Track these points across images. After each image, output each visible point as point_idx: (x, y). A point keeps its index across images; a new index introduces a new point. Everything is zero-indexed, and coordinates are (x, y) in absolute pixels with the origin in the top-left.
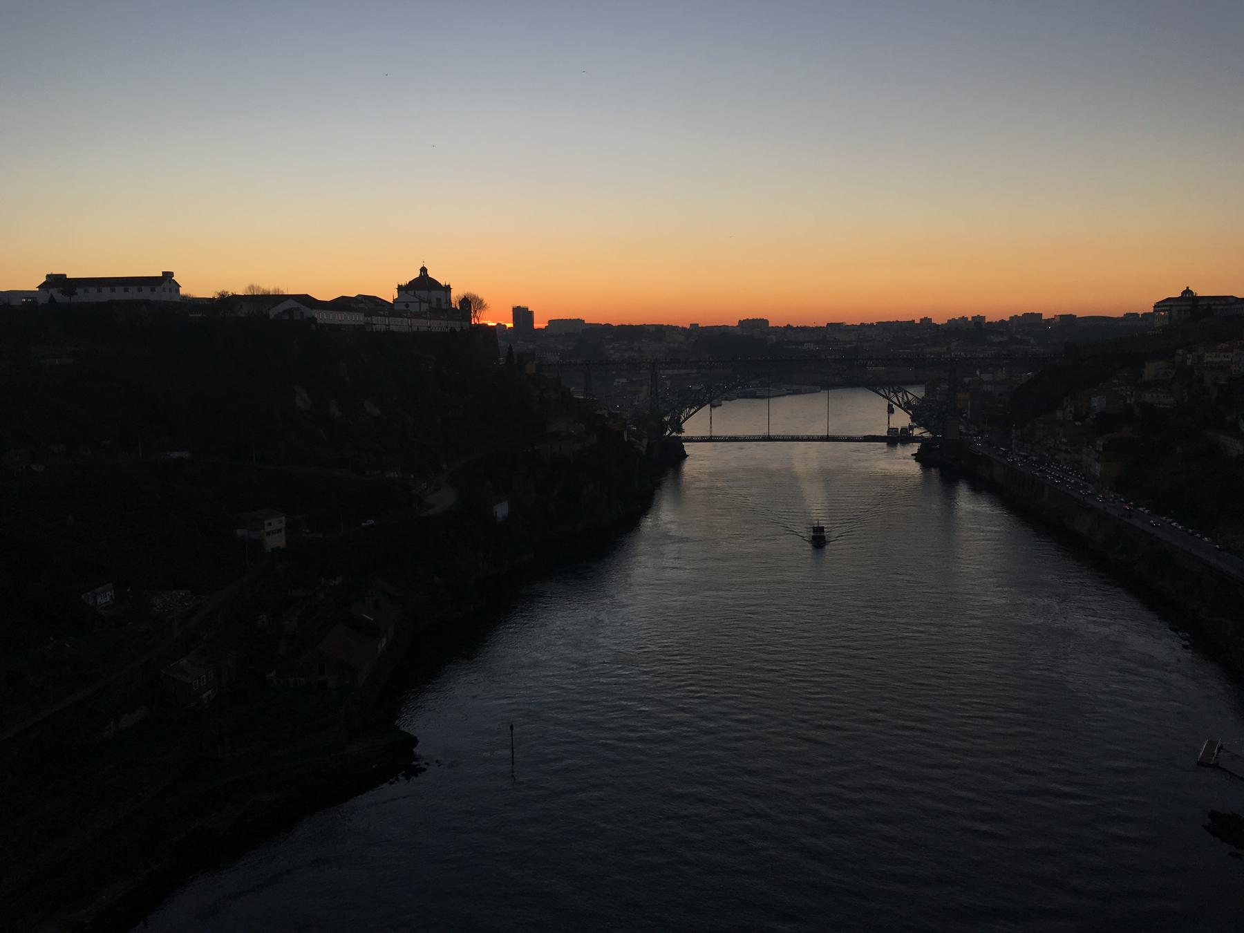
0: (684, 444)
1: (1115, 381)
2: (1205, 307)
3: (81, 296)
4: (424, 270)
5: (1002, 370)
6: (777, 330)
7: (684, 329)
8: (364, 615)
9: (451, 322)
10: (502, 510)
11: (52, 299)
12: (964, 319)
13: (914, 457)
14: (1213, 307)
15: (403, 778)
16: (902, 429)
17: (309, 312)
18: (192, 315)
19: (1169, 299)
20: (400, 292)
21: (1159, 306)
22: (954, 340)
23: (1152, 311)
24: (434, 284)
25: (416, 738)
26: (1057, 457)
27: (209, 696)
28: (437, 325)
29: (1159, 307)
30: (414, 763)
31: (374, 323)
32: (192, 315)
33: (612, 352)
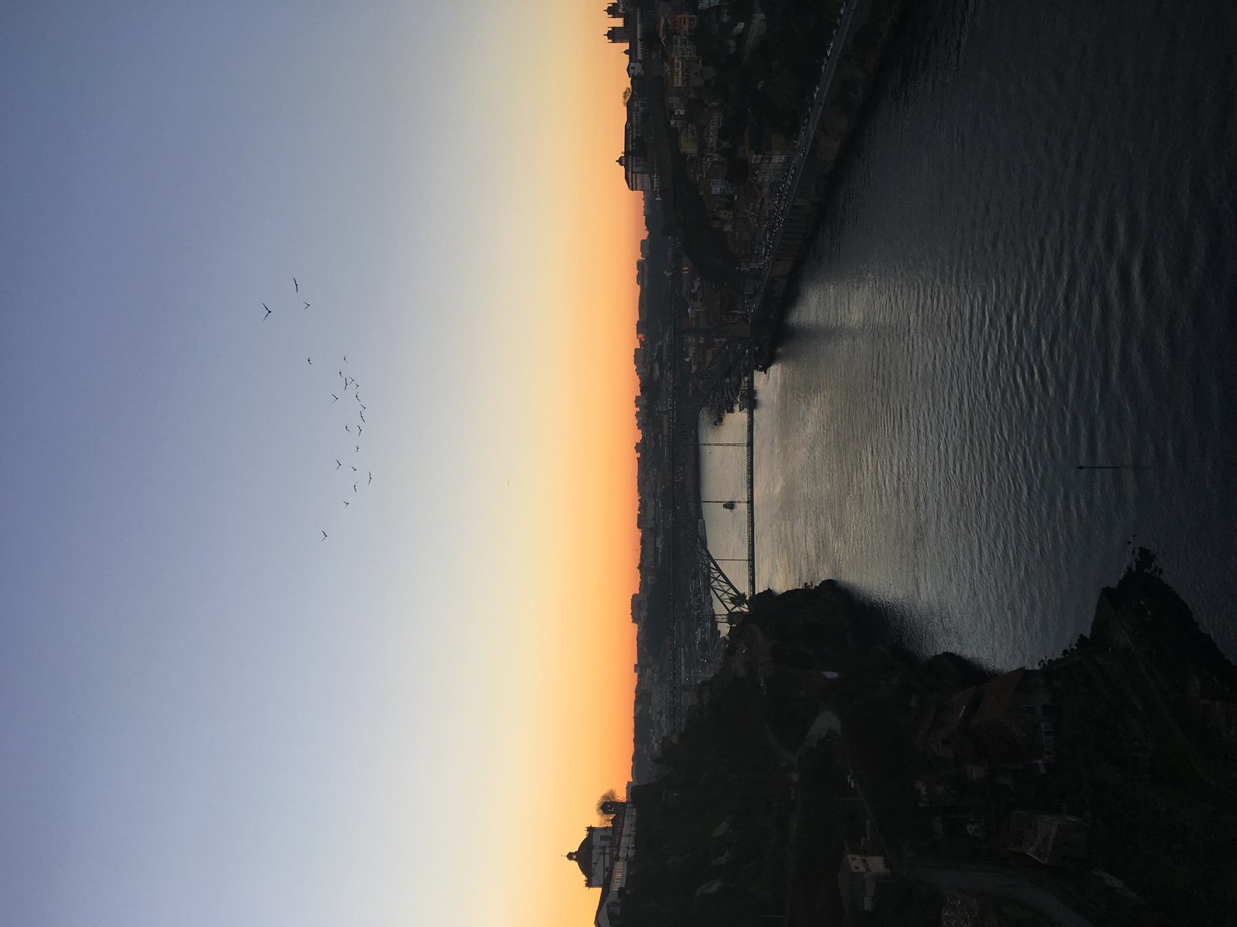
0: (756, 593)
1: (698, 179)
2: (634, 144)
4: (570, 856)
6: (644, 585)
7: (641, 676)
10: (831, 675)
12: (638, 415)
14: (634, 138)
15: (1153, 564)
19: (627, 178)
21: (632, 187)
24: (586, 845)
26: (767, 215)
28: (628, 829)
29: (632, 182)
31: (625, 855)
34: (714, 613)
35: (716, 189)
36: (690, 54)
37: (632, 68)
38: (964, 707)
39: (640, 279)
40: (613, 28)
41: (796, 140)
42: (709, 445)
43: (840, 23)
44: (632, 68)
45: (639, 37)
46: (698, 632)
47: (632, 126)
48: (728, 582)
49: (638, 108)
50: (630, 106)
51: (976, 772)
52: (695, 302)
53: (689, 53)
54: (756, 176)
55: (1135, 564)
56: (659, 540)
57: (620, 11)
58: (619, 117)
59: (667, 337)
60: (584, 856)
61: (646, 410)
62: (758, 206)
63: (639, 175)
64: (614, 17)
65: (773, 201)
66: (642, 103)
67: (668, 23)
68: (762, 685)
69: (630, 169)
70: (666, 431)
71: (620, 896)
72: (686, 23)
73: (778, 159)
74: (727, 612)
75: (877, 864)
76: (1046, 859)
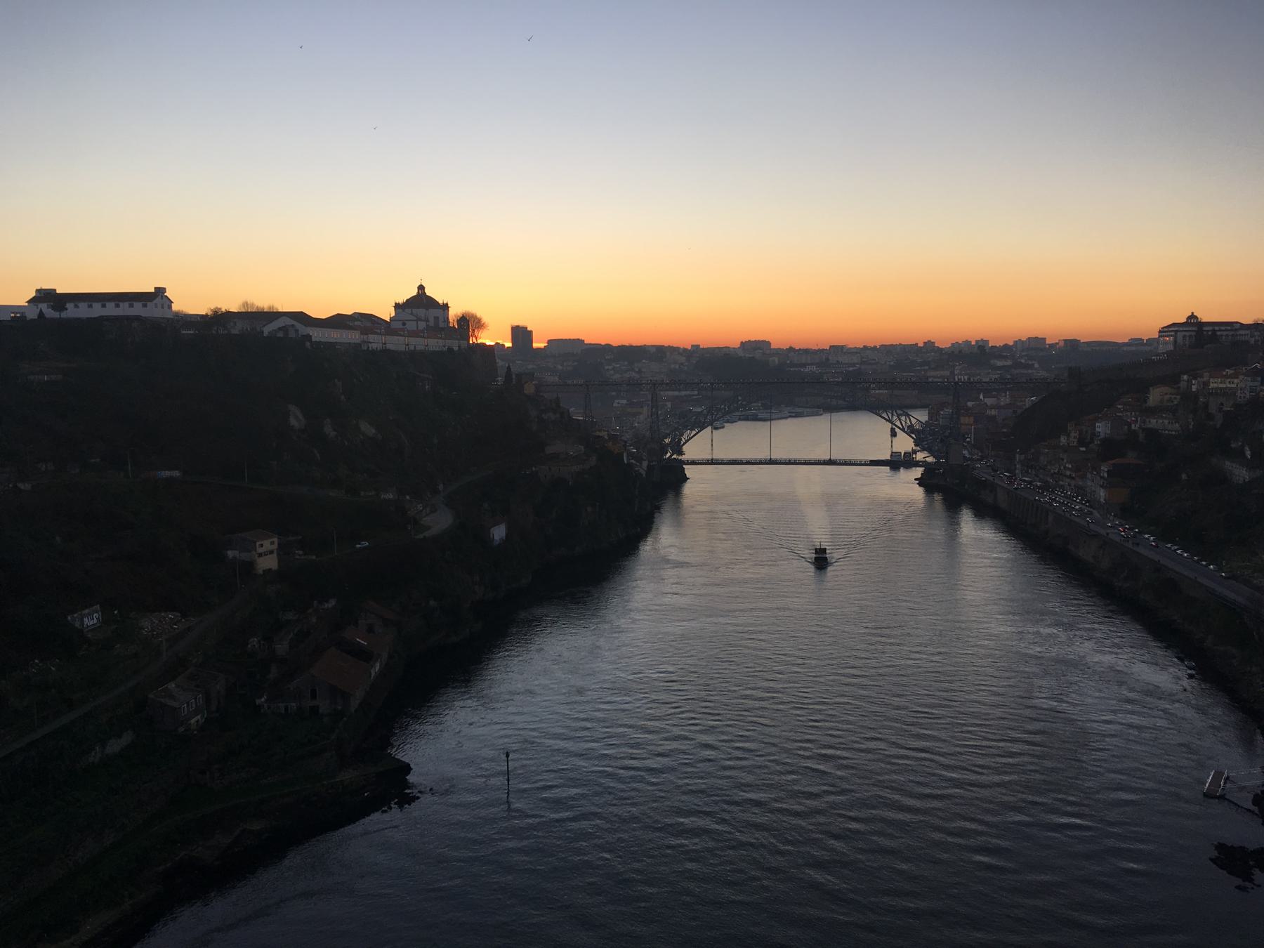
1: (1119, 407)
2: (1210, 333)
3: (71, 312)
4: (421, 288)
5: (1006, 393)
6: (778, 352)
7: (685, 350)
8: (358, 640)
9: (449, 341)
10: (499, 533)
11: (41, 314)
12: (967, 343)
13: (918, 482)
14: (1218, 333)
16: (905, 453)
17: (304, 330)
18: (184, 332)
19: (1174, 325)
20: (397, 310)
21: (1164, 331)
22: (957, 364)
23: (1157, 337)
24: (431, 303)
25: (408, 765)
26: (1061, 483)
27: (197, 721)
28: (435, 344)
30: (406, 791)
31: (371, 341)
32: (184, 332)
33: (612, 372)
41: (1114, 516)
43: (1202, 565)
47: (1236, 330)
53: (1242, 396)
56: (814, 368)
59: (1043, 374)
60: (421, 301)
62: (1068, 473)
66: (1258, 341)
68: (534, 469)
70: (929, 374)
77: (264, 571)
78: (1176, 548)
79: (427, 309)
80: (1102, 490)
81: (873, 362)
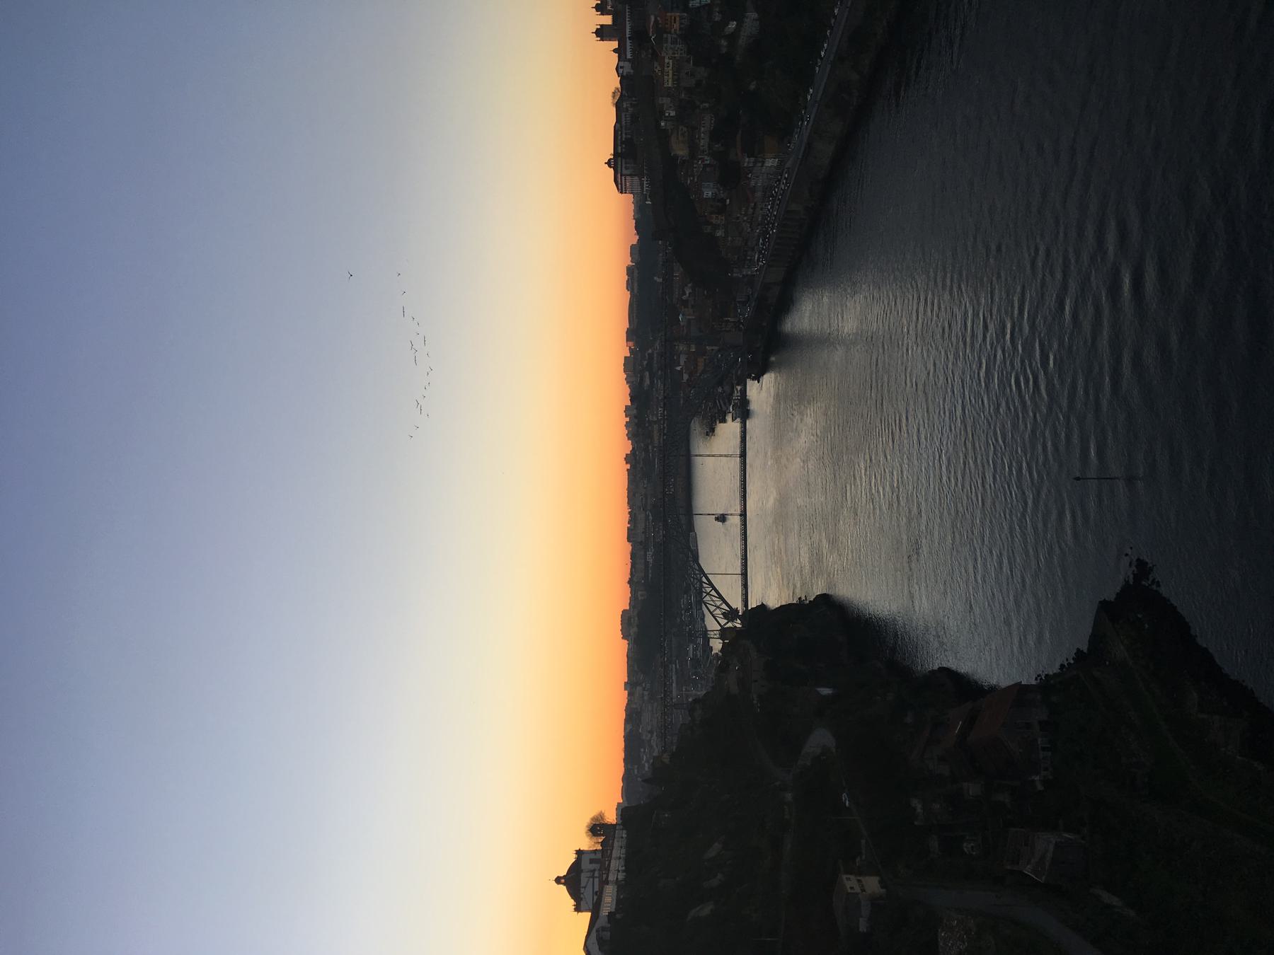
0: (749, 608)
1: (689, 182)
2: (624, 146)
4: (558, 880)
7: (629, 695)
10: (826, 691)
12: (627, 425)
14: (623, 140)
19: (616, 181)
20: (582, 909)
24: (575, 869)
28: (618, 851)
29: (621, 184)
31: (615, 879)
34: (706, 628)
35: (708, 193)
36: (681, 54)
37: (621, 67)
38: (960, 723)
39: (630, 286)
40: (602, 26)
42: (700, 456)
44: (621, 67)
45: (628, 36)
46: (691, 648)
47: (621, 127)
48: (720, 597)
49: (627, 109)
50: (618, 106)
51: (973, 789)
52: (686, 309)
53: (679, 52)
54: (748, 179)
55: (1131, 576)
56: (650, 553)
57: (609, 8)
58: (609, 117)
59: (657, 345)
60: (572, 880)
61: (636, 421)
62: (751, 211)
63: (628, 178)
64: (602, 14)
65: (765, 205)
66: (631, 104)
67: (658, 21)
68: (755, 702)
69: (619, 171)
71: (609, 922)
72: (677, 21)
73: (771, 162)
74: (719, 628)
75: (872, 884)
76: (1044, 878)
77: (882, 888)
78: (819, 60)
79: (582, 871)
80: (766, 165)
81: (644, 500)
